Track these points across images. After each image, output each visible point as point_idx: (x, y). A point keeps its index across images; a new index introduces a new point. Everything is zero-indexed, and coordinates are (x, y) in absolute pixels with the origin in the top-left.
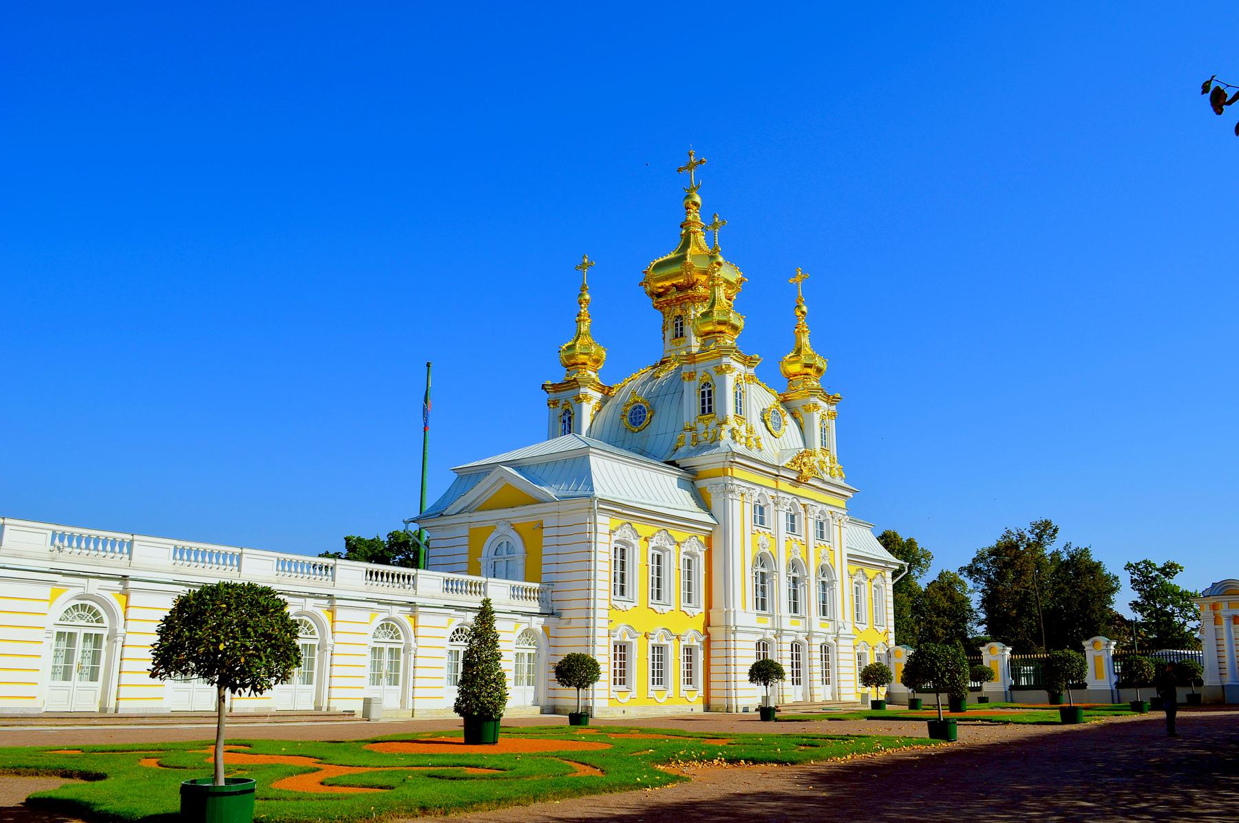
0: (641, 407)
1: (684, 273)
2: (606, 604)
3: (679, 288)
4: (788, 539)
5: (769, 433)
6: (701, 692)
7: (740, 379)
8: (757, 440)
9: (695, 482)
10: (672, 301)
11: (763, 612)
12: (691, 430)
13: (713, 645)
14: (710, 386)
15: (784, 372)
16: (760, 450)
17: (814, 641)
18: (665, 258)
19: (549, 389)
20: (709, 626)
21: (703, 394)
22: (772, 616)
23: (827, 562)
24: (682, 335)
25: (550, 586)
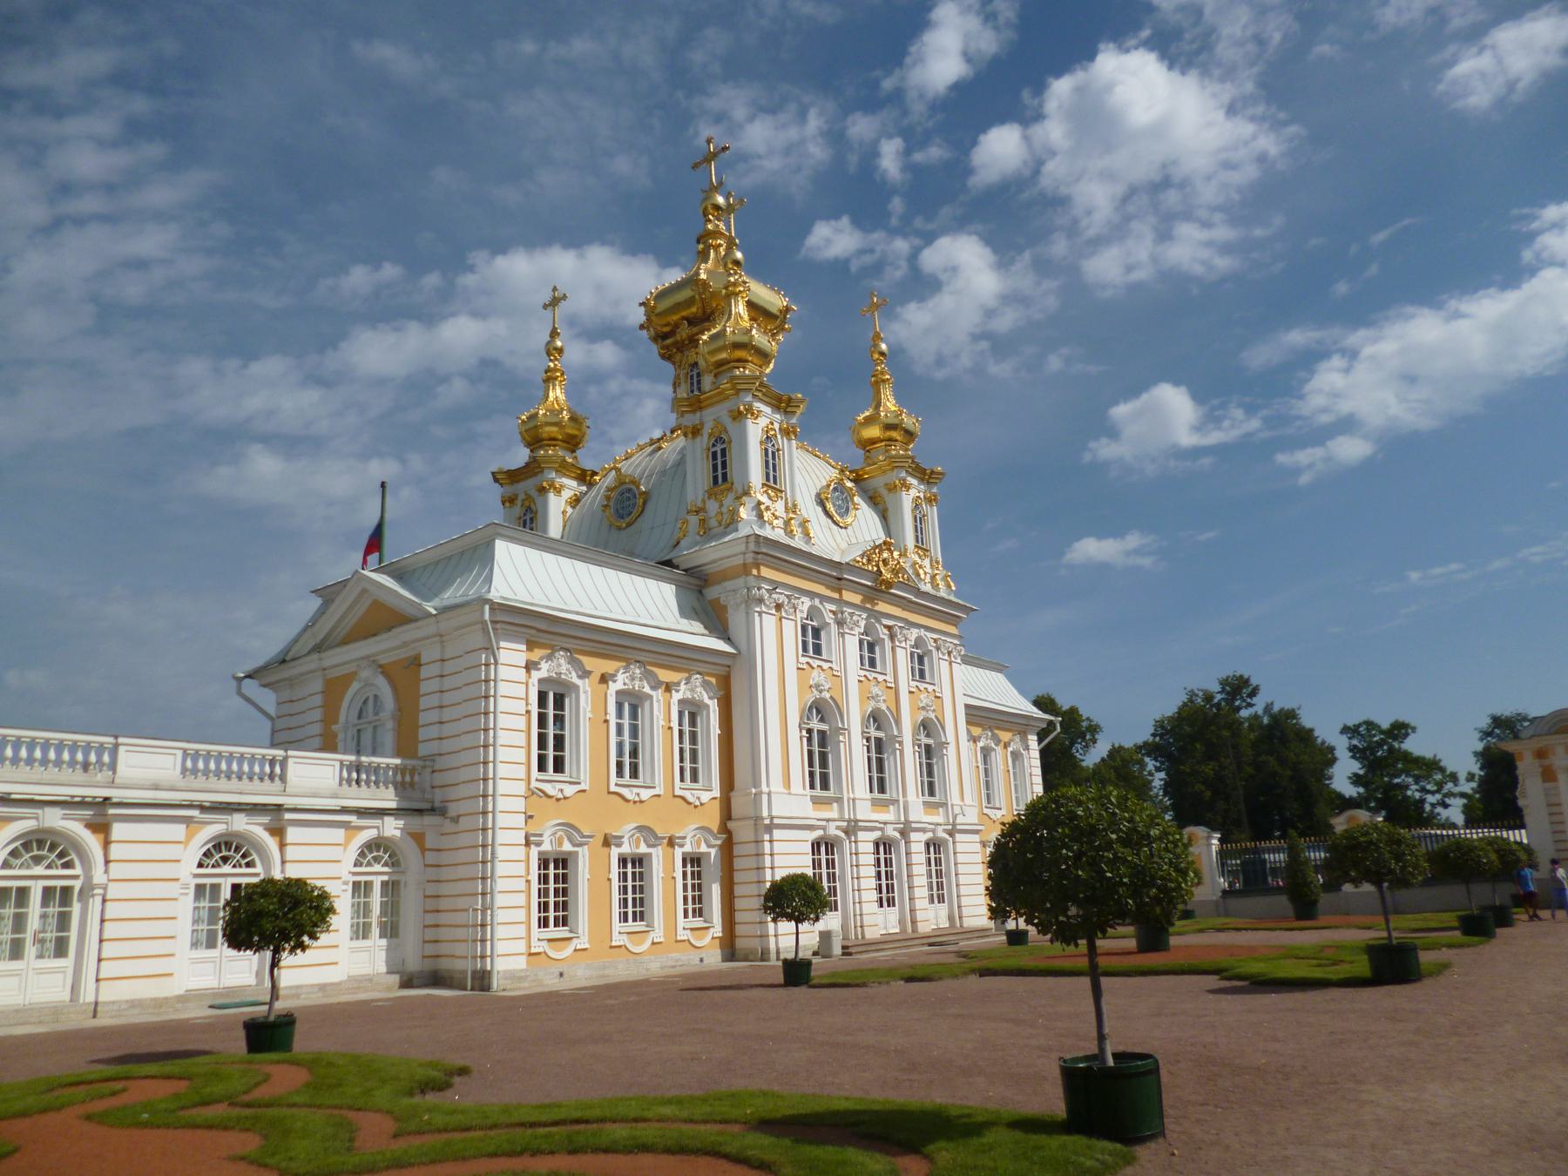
0: (629, 490)
3: (691, 321)
5: (830, 521)
6: (717, 930)
8: (804, 524)
9: (704, 591)
10: (683, 341)
11: (825, 794)
12: (697, 512)
13: (737, 850)
14: (724, 442)
16: (806, 534)
17: (914, 836)
19: (502, 479)
20: (729, 818)
21: (714, 454)
22: (839, 800)
23: (932, 716)
25: (427, 763)
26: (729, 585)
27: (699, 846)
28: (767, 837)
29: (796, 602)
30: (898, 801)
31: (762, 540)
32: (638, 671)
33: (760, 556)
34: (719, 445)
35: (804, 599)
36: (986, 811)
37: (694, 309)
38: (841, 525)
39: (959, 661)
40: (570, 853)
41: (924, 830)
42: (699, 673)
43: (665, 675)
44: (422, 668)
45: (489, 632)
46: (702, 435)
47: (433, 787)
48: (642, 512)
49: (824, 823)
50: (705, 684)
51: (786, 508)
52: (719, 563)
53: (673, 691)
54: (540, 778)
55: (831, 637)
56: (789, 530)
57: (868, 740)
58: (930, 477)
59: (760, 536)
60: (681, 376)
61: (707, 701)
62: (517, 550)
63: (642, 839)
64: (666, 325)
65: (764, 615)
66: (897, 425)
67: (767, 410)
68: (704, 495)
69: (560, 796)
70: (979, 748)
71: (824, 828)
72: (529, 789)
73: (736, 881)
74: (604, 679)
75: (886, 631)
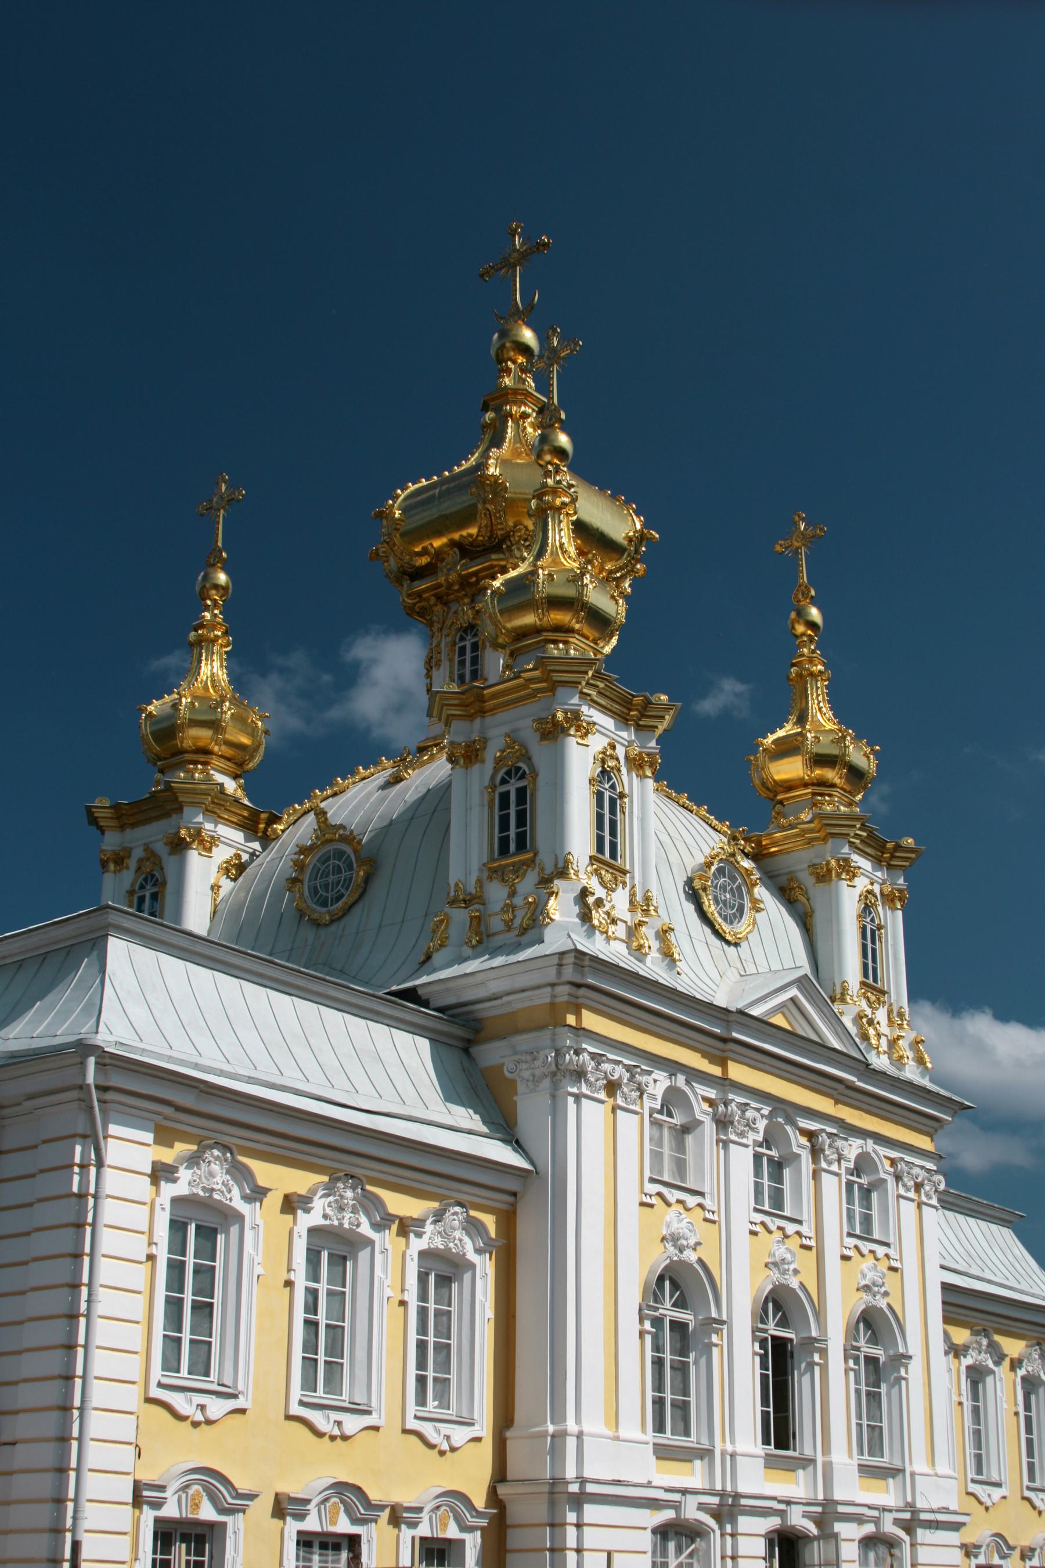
0: (340, 854)
1: (480, 506)
3: (467, 550)
4: (758, 1228)
5: (708, 931)
7: (612, 757)
8: (664, 934)
9: (473, 1050)
10: (450, 586)
12: (468, 902)
13: (515, 1539)
14: (523, 776)
15: (764, 784)
16: (667, 954)
21: (505, 797)
23: (882, 1303)
26: (523, 1041)
27: (445, 1526)
28: (571, 1517)
29: (644, 1079)
30: (812, 1461)
31: (587, 963)
32: (349, 1194)
33: (582, 991)
34: (513, 781)
35: (660, 1075)
36: (973, 1488)
37: (474, 531)
38: (728, 937)
39: (934, 1201)
40: (211, 1525)
43: (399, 1204)
45: (92, 1108)
46: (483, 761)
49: (676, 1497)
50: (473, 1227)
51: (632, 902)
52: (506, 999)
53: (412, 1235)
54: (165, 1381)
56: (635, 944)
57: (763, 1343)
59: (584, 954)
60: (443, 645)
61: (472, 1256)
62: (145, 956)
63: (342, 1508)
64: (420, 554)
65: (583, 1100)
66: (836, 757)
67: (607, 722)
68: (481, 870)
69: (199, 1417)
70: (963, 1369)
71: (676, 1506)
74: (291, 1204)
75: (804, 1141)
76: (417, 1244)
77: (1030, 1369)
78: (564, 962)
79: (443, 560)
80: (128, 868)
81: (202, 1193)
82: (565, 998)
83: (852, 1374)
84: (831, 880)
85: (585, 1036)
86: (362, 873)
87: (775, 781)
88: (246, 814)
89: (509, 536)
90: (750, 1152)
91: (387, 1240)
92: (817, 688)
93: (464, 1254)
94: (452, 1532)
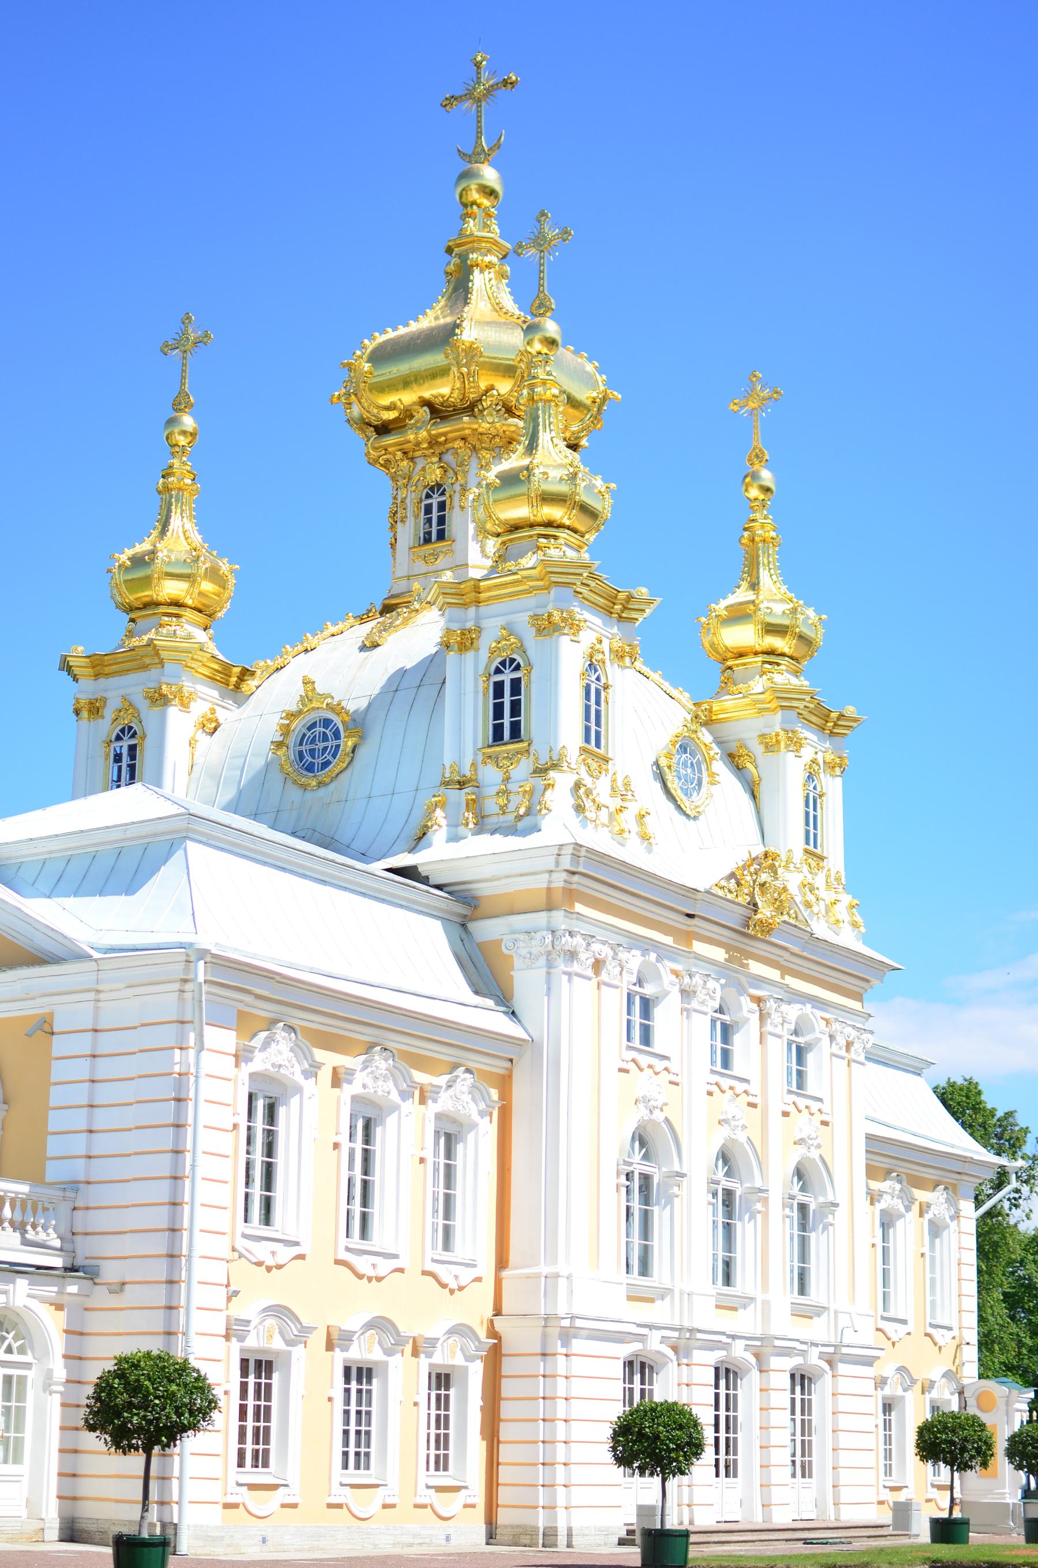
2: (221, 1247)
3: (437, 411)
4: (715, 1088)
5: (672, 806)
6: (477, 1492)
7: (598, 651)
9: (471, 926)
12: (462, 784)
13: (508, 1366)
14: (518, 668)
15: (712, 645)
17: (775, 1362)
18: (402, 331)
21: (499, 688)
23: (814, 1154)
24: (441, 536)
32: (383, 1065)
33: (576, 878)
39: (862, 1058)
40: (278, 1353)
41: (711, 1346)
42: (468, 1071)
44: (54, 1037)
46: (477, 650)
47: (73, 1234)
48: (352, 760)
51: (613, 789)
52: (504, 881)
55: (663, 1017)
58: (836, 725)
60: (408, 501)
61: (476, 1117)
64: (388, 408)
66: (787, 627)
68: (475, 754)
71: (641, 1338)
72: (234, 1250)
73: (503, 1415)
75: (755, 1006)
76: (433, 1108)
77: (936, 1212)
78: (562, 852)
79: (412, 417)
80: (103, 717)
81: (272, 1069)
82: (561, 884)
83: (788, 1220)
84: (779, 750)
85: (577, 919)
86: (350, 743)
87: (726, 648)
88: (216, 667)
89: (481, 400)
90: (708, 1019)
91: (410, 1106)
92: (769, 555)
93: (470, 1116)
94: (459, 1360)
